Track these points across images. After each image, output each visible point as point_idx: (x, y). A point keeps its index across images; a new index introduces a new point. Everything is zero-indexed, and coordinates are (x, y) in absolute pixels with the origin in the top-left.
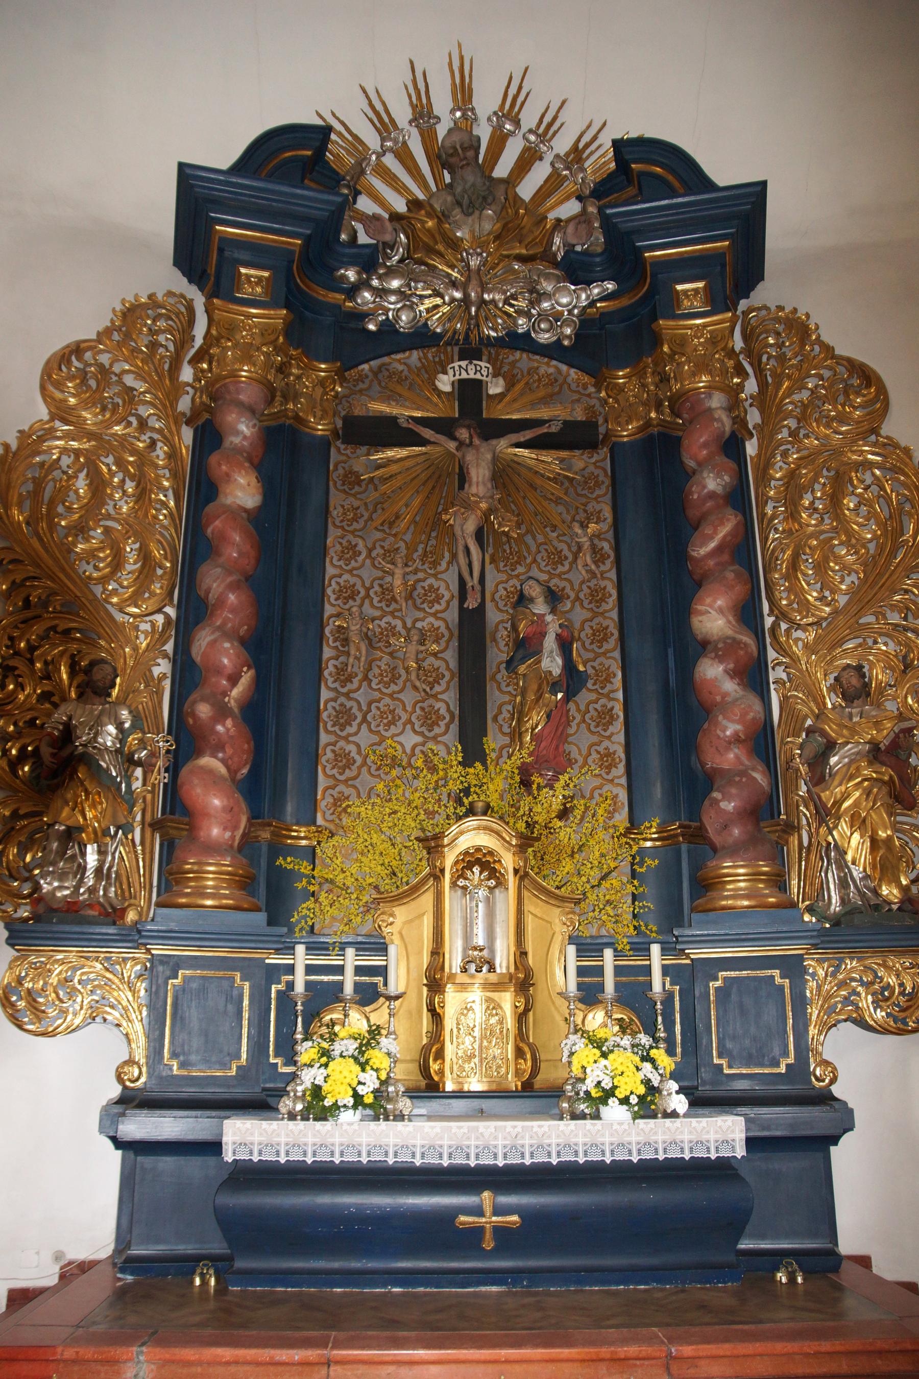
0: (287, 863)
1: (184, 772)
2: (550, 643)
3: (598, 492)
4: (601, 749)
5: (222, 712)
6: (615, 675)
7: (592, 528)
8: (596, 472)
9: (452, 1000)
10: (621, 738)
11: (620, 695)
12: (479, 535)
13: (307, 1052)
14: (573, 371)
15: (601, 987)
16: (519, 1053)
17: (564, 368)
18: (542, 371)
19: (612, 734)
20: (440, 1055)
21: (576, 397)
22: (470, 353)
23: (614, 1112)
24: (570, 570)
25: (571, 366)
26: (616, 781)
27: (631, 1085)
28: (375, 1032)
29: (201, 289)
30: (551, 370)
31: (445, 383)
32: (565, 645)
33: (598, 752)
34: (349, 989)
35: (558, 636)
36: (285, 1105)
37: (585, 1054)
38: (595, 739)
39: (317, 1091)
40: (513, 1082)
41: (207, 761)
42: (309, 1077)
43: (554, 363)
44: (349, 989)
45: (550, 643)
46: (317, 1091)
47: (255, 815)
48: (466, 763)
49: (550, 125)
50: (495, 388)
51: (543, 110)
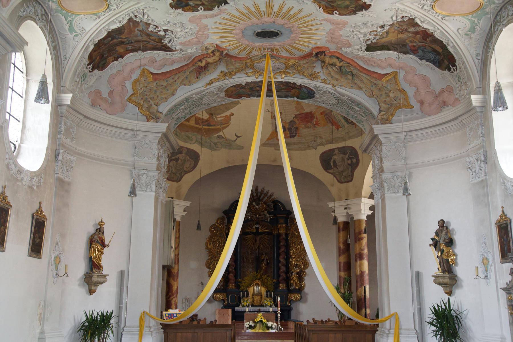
0: (239, 284)
1: (229, 275)
2: (265, 260)
5: (232, 269)
7: (271, 246)
9: (254, 297)
12: (258, 248)
13: (242, 301)
15: (268, 296)
16: (261, 302)
20: (254, 302)
22: (257, 223)
23: (268, 307)
27: (269, 304)
28: (248, 300)
29: (226, 216)
31: (254, 227)
32: (267, 260)
34: (245, 296)
35: (266, 259)
36: (240, 306)
37: (266, 302)
39: (243, 305)
40: (260, 305)
41: (231, 274)
42: (242, 304)
44: (245, 296)
45: (265, 260)
46: (243, 305)
47: (235, 278)
48: (256, 273)
50: (260, 228)
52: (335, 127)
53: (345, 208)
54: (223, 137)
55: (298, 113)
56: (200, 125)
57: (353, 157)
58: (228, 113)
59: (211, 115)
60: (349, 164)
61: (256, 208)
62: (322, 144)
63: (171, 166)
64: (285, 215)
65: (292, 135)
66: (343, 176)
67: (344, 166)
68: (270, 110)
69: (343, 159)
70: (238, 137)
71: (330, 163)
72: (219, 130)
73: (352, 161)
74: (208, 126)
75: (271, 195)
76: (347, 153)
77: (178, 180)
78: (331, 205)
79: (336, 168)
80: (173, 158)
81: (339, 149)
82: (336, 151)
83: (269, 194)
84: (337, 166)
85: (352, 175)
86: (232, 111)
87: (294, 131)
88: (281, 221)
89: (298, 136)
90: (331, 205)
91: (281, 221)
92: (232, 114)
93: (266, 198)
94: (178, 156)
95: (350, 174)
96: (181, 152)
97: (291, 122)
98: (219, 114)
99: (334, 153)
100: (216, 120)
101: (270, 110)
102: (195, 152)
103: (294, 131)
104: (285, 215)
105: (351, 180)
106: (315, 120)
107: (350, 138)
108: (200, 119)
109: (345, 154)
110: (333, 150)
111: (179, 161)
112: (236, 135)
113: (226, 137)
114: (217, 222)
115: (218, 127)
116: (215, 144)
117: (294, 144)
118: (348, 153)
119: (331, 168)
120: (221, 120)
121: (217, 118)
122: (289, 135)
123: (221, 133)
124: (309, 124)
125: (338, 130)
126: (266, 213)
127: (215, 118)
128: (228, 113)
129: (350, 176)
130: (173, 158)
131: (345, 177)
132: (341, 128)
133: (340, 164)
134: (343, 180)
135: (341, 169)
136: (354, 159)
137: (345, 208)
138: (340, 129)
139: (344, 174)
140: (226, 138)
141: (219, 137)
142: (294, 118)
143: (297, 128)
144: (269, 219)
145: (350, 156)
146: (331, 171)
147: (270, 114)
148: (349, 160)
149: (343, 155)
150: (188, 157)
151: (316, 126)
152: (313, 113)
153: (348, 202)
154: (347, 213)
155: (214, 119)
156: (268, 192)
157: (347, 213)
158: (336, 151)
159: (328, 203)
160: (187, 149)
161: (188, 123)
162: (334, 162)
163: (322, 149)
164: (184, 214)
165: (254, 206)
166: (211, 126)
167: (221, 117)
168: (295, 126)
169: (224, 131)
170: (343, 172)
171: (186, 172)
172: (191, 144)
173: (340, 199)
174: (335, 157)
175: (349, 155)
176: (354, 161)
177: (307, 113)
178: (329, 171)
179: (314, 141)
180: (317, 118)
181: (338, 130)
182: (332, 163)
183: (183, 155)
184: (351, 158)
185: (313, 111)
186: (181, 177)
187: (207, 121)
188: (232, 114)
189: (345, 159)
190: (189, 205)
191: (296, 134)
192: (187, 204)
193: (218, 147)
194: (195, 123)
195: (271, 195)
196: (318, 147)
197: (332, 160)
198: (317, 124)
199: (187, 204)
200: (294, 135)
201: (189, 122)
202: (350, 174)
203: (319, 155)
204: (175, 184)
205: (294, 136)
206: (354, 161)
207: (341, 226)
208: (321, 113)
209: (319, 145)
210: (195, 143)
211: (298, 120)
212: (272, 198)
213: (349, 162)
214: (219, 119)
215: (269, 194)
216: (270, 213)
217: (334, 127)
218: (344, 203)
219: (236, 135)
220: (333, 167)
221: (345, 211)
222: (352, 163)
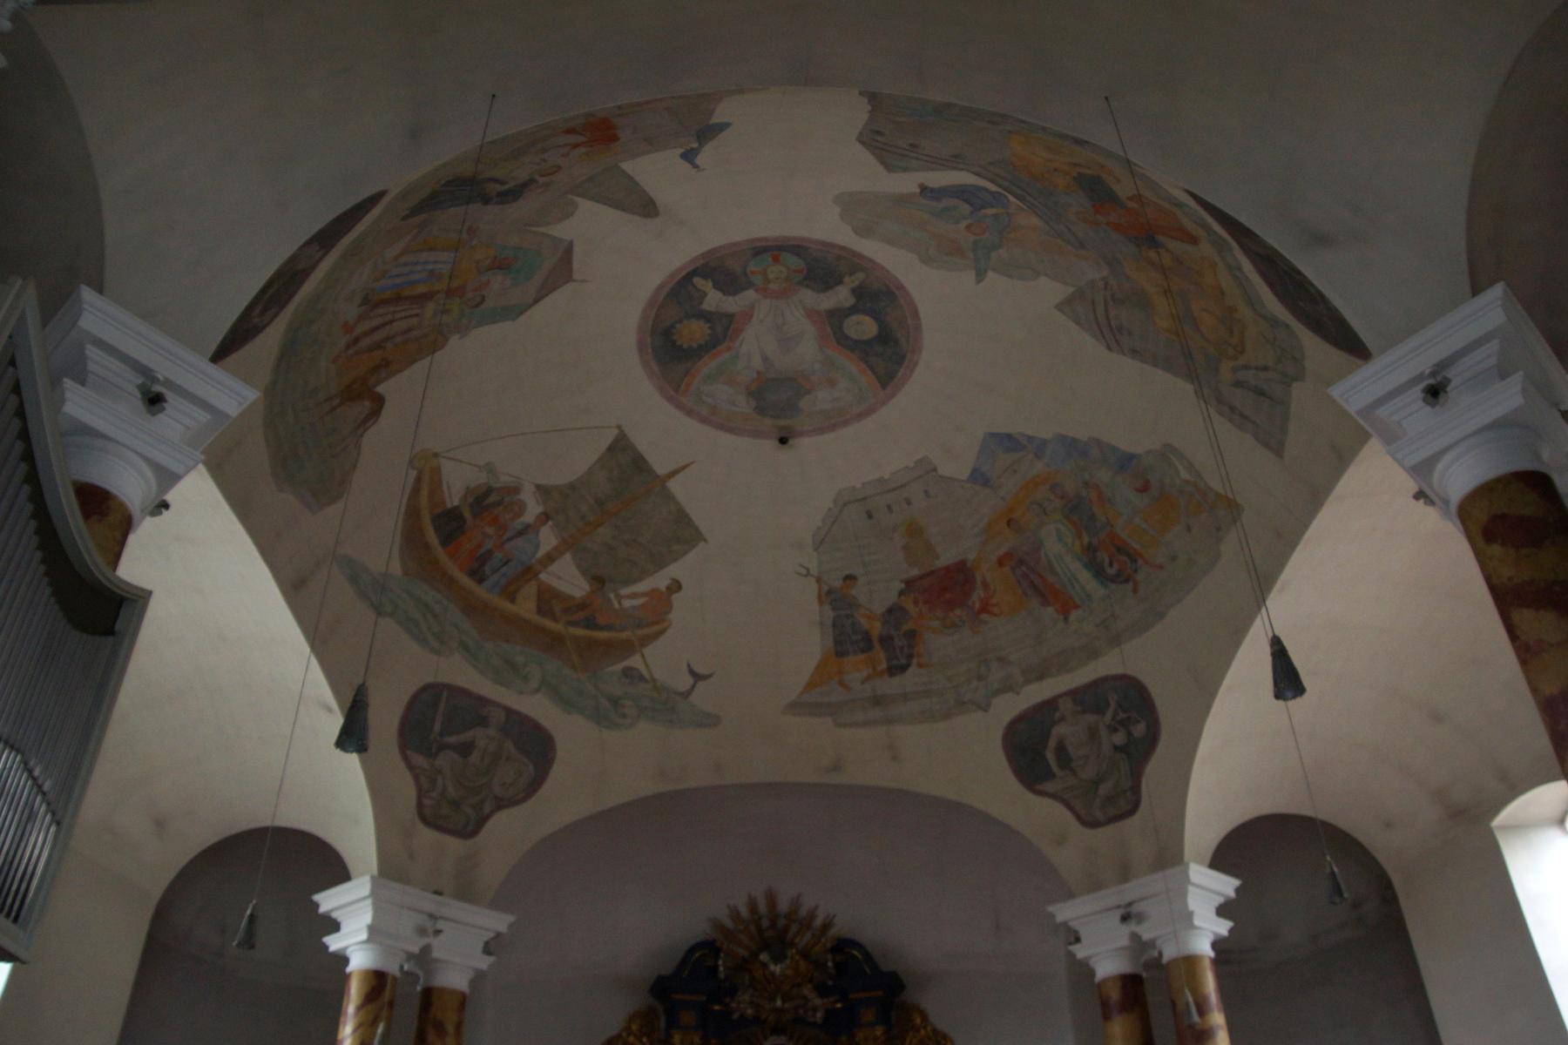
52: (1057, 611)
53: (1125, 918)
54: (642, 678)
55: (915, 572)
56: (556, 620)
58: (660, 581)
59: (599, 581)
60: (1116, 748)
61: (773, 974)
62: (1008, 687)
63: (440, 772)
64: (880, 993)
65: (895, 662)
68: (814, 571)
69: (1093, 733)
70: (697, 677)
72: (628, 648)
73: (1129, 734)
74: (587, 627)
75: (826, 926)
76: (1108, 705)
77: (468, 831)
78: (1064, 912)
80: (452, 739)
81: (1073, 694)
82: (1066, 706)
83: (818, 922)
85: (1136, 789)
86: (674, 570)
87: (902, 648)
88: (868, 1015)
89: (920, 666)
90: (1064, 912)
91: (868, 1015)
92: (676, 586)
93: (808, 936)
94: (469, 734)
96: (483, 722)
97: (890, 611)
98: (628, 582)
99: (1058, 715)
100: (616, 605)
101: (814, 571)
102: (537, 727)
103: (902, 648)
104: (880, 993)
105: (1134, 808)
106: (978, 595)
107: (1116, 640)
108: (558, 595)
109: (1099, 710)
110: (1051, 704)
111: (475, 757)
112: (692, 673)
113: (656, 676)
114: (628, 1029)
115: (624, 635)
116: (615, 702)
117: (905, 697)
118: (1113, 704)
119: (1050, 775)
120: (634, 607)
121: (619, 598)
122: (884, 666)
123: (635, 661)
124: (958, 612)
125: (1066, 619)
126: (807, 991)
127: (612, 596)
128: (660, 581)
130: (452, 739)
132: (1077, 607)
134: (1099, 815)
137: (1125, 918)
138: (1074, 615)
139: (1104, 789)
140: (654, 680)
141: (628, 673)
142: (901, 593)
143: (912, 635)
144: (819, 1015)
145: (1122, 715)
146: (1050, 786)
147: (814, 586)
148: (1116, 730)
149: (1091, 718)
150: (509, 746)
151: (984, 616)
152: (969, 564)
153: (1131, 890)
154: (1135, 937)
155: (609, 600)
156: (812, 915)
157: (1135, 937)
158: (1066, 706)
159: (1051, 909)
160: (509, 711)
161: (507, 606)
162: (1061, 750)
163: (1009, 707)
164: (484, 963)
165: (765, 965)
166: (601, 628)
167: (634, 596)
168: (905, 628)
169: (647, 651)
170: (1096, 783)
171: (501, 804)
172: (521, 693)
173: (1096, 885)
174: (1060, 730)
175: (1115, 714)
176: (1139, 729)
177: (948, 569)
178: (1040, 787)
179: (980, 678)
180: (985, 585)
181: (1066, 619)
182: (1050, 755)
183: (492, 732)
184: (1125, 723)
185: (971, 557)
186: (482, 821)
187: (583, 605)
188: (676, 586)
190: (503, 928)
191: (910, 656)
192: (499, 922)
193: (624, 716)
194: (540, 611)
195: (826, 926)
196: (995, 701)
197: (1052, 743)
198: (985, 608)
199: (499, 922)
200: (903, 661)
201: (513, 600)
203: (998, 735)
204: (454, 844)
205: (903, 669)
206: (1139, 729)
207: (1115, 994)
208: (1001, 562)
209: (997, 693)
210: (537, 691)
211: (916, 603)
212: (833, 932)
213: (1119, 738)
214: (627, 603)
215: (818, 922)
216: (823, 991)
217: (1050, 609)
218: (1113, 896)
219: (692, 673)
220: (1055, 768)
221: (1126, 930)
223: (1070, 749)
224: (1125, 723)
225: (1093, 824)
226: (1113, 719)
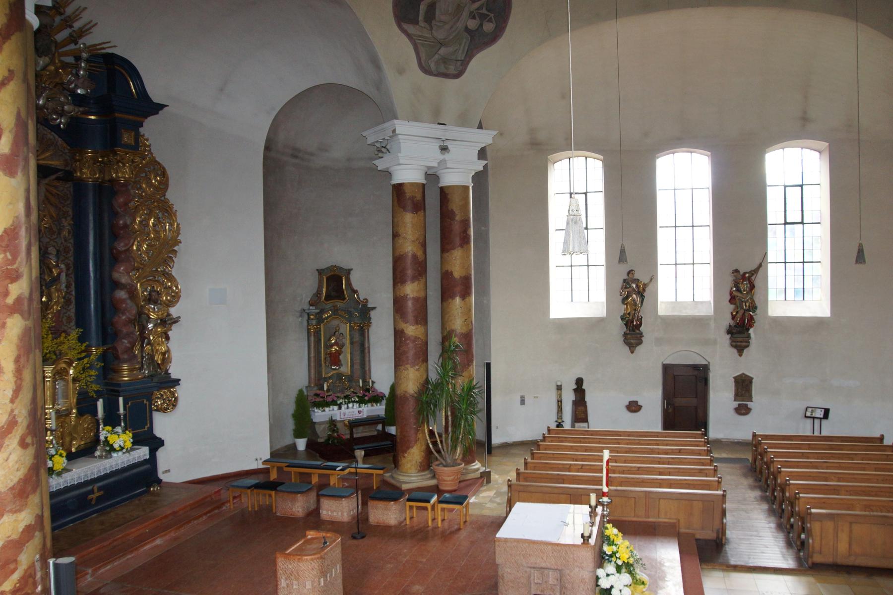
3: (68, 202)
4: (67, 315)
6: (72, 285)
8: (68, 192)
10: (73, 310)
11: (74, 293)
14: (60, 139)
17: (57, 137)
18: (49, 136)
19: (71, 309)
21: (61, 153)
24: (57, 238)
25: (60, 137)
26: (72, 328)
30: (52, 137)
33: (66, 316)
38: (65, 311)
43: (53, 133)
49: (77, 16)
51: (105, 41)
57: (492, 15)
60: (467, 29)
66: (437, 56)
67: (452, 27)
71: (419, 6)
73: (481, 25)
79: (427, 26)
83: (77, 25)
84: (433, 22)
85: (465, 63)
95: (459, 59)
105: (458, 76)
119: (415, 22)
129: (459, 63)
131: (445, 60)
133: (443, 18)
134: (433, 66)
135: (440, 35)
136: (490, 21)
139: (443, 51)
145: (484, 11)
146: (411, 29)
148: (474, 18)
156: (76, 16)
170: (442, 44)
178: (405, 26)
189: (465, 14)
202: (461, 56)
206: (489, 27)
213: (472, 24)
215: (77, 25)
220: (421, 18)
222: (477, 29)
223: (437, 12)
224: (483, 17)
225: (426, 71)
226: (478, 9)
